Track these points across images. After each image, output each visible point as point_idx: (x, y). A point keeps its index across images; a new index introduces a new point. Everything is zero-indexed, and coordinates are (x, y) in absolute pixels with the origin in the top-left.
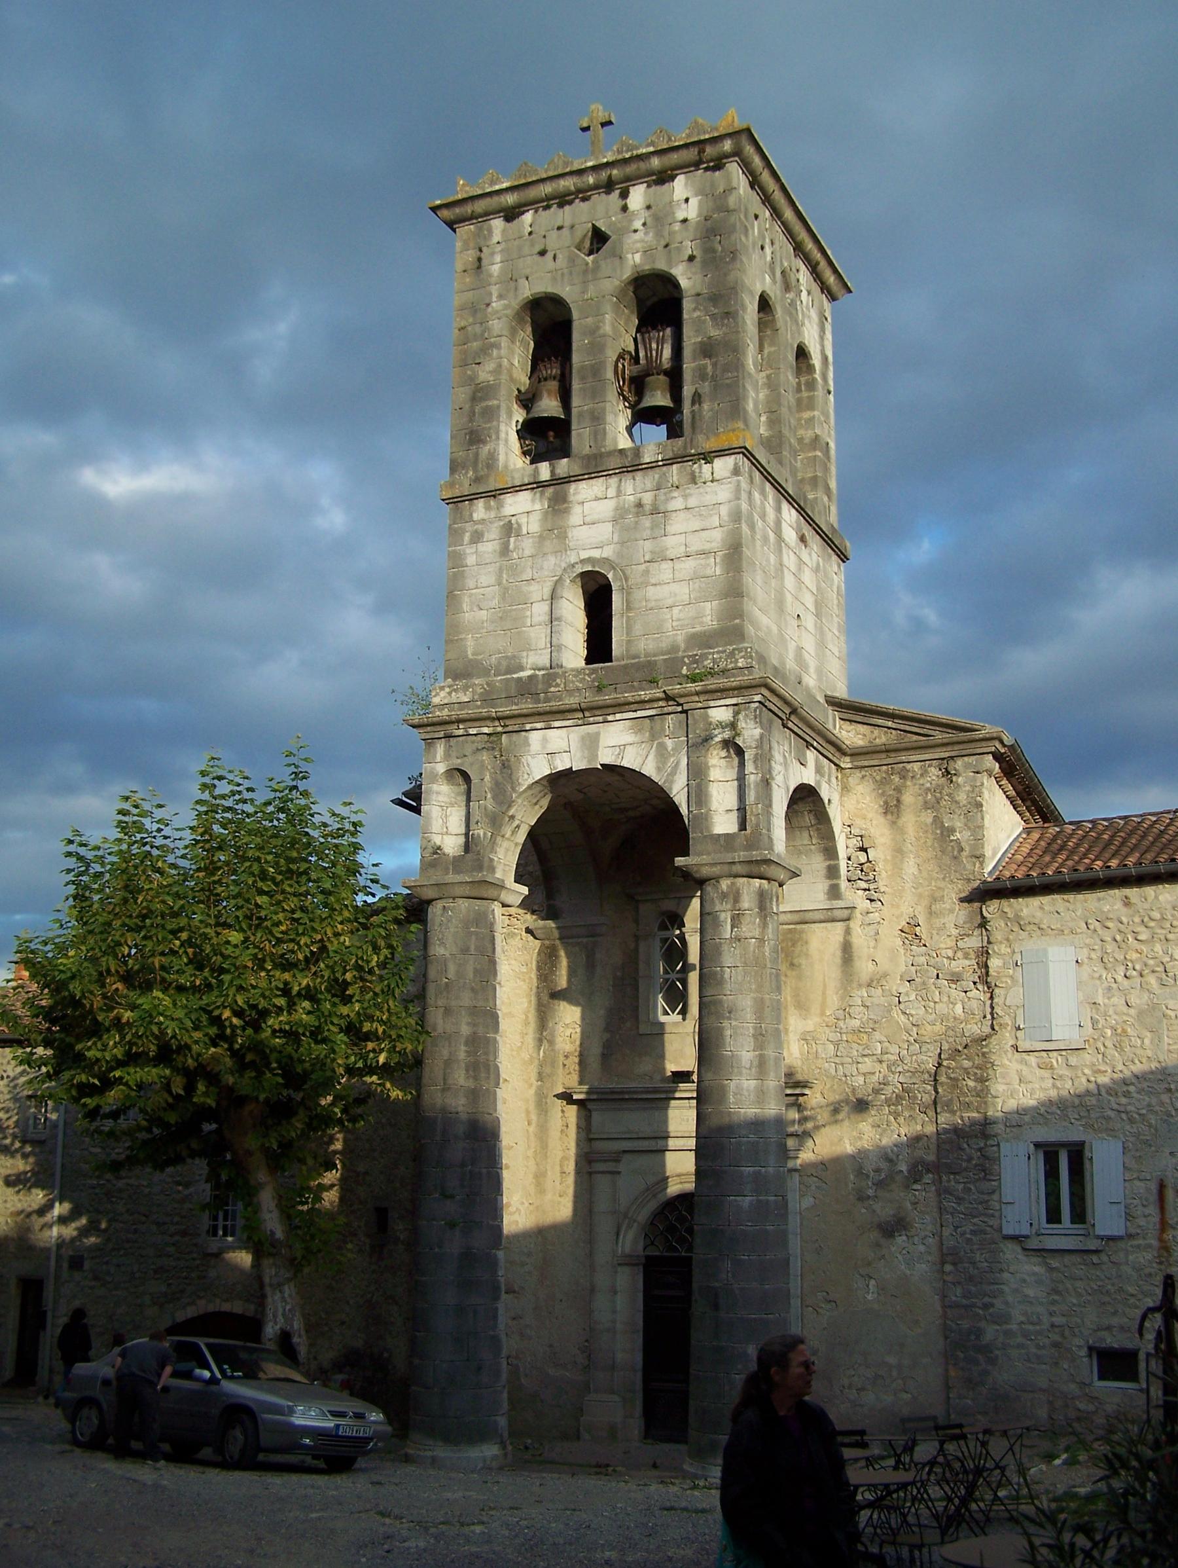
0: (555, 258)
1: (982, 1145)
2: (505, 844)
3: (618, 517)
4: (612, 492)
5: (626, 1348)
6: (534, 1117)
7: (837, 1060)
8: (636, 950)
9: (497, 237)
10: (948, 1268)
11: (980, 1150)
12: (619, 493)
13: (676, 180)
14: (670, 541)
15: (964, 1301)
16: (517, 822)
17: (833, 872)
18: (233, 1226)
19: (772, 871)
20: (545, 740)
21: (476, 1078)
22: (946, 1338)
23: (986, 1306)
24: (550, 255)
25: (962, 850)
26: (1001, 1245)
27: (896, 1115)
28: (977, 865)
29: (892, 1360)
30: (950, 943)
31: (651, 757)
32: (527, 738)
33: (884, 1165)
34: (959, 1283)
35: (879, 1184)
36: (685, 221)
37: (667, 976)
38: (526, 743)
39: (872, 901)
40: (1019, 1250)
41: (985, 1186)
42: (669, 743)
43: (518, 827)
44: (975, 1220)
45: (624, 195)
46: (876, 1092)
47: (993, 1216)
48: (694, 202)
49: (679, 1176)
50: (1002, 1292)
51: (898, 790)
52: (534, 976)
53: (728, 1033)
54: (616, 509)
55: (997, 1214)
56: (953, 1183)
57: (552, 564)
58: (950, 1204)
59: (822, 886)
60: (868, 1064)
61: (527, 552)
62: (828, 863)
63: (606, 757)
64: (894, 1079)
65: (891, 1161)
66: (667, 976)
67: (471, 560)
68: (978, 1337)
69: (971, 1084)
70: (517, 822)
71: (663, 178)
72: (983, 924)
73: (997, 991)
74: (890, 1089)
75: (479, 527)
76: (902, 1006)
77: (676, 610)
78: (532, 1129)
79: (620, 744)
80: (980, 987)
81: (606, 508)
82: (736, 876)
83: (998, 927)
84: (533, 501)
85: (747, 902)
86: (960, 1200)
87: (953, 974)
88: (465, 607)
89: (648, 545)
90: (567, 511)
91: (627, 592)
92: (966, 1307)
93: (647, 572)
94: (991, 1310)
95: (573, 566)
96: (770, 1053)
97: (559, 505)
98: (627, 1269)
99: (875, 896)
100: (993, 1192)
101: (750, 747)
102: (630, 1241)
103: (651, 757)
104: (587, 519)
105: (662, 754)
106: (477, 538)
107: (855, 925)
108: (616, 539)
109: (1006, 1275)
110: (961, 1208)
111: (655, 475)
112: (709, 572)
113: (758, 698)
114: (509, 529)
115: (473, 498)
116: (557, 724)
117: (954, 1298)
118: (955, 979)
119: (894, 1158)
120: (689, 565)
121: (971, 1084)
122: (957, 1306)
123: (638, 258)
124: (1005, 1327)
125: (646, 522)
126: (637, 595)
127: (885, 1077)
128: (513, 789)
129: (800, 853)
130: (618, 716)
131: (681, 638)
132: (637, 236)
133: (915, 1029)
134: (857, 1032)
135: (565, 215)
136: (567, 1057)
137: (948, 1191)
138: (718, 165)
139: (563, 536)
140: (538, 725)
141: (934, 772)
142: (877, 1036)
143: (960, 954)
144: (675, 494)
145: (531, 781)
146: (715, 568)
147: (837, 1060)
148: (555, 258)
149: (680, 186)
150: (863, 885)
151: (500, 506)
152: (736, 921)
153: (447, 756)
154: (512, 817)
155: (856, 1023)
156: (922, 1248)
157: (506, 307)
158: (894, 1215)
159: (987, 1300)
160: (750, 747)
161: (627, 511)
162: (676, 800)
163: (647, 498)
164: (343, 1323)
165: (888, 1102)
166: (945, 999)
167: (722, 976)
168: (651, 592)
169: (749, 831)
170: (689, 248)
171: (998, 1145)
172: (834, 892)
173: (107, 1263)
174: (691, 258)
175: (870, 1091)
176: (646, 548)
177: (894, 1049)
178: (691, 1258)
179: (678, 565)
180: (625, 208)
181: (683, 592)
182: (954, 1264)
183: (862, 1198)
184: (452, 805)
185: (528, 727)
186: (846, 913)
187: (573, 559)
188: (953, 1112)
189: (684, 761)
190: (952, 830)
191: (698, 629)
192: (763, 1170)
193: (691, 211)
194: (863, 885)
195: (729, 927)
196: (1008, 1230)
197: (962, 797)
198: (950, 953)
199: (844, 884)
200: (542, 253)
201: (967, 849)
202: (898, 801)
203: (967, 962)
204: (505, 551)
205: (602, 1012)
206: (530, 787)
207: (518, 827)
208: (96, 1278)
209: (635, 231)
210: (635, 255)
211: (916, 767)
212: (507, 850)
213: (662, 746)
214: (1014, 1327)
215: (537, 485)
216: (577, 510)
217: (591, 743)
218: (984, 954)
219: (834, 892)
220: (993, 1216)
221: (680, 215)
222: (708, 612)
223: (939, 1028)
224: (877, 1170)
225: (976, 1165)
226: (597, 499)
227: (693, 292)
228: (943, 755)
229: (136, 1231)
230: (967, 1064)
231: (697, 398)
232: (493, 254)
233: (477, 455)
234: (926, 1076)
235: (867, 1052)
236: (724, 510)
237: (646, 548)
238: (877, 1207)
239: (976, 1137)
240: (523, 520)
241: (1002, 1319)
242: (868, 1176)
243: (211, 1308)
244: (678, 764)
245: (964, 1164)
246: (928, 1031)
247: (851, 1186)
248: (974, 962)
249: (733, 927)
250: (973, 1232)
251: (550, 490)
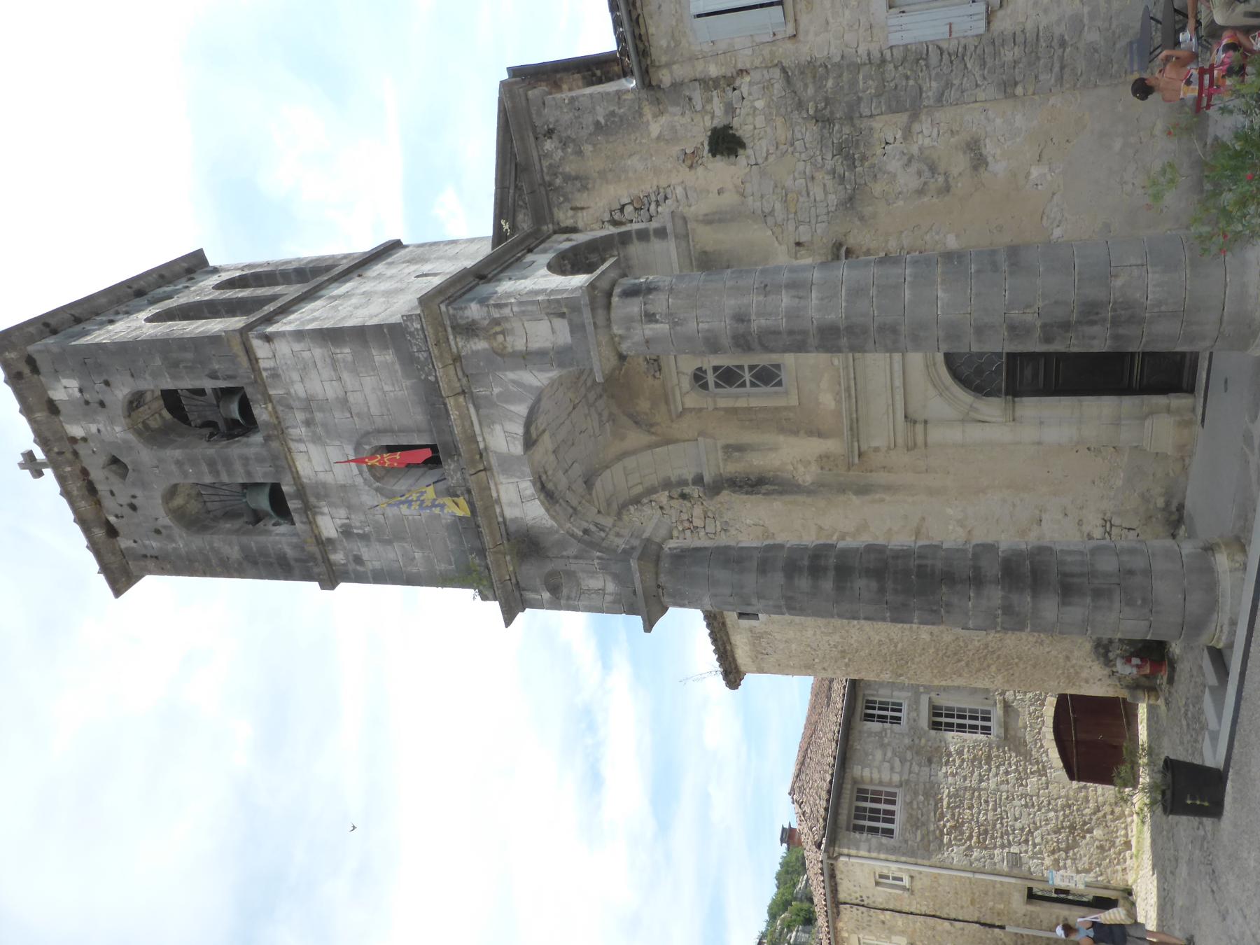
0: (134, 497)
1: (891, 66)
2: (611, 537)
3: (316, 439)
4: (302, 447)
5: (1099, 410)
6: (877, 496)
7: (813, 221)
8: (727, 410)
9: (130, 543)
10: (1019, 90)
11: (896, 68)
12: (300, 441)
13: (54, 398)
14: (330, 394)
15: (1056, 69)
16: (593, 528)
17: (643, 235)
18: (983, 712)
19: (604, 284)
20: (511, 504)
21: (825, 569)
22: (1096, 86)
23: (1063, 44)
24: (134, 501)
25: (613, 114)
26: (996, 34)
27: (864, 158)
28: (625, 97)
29: (1118, 144)
30: (698, 118)
31: (512, 408)
32: (512, 520)
33: (915, 167)
34: (1036, 77)
35: (933, 169)
36: (81, 391)
37: (748, 383)
38: (515, 520)
39: (666, 198)
40: (1000, 14)
41: (934, 59)
42: (496, 390)
43: (596, 525)
44: (969, 65)
45: (73, 440)
46: (842, 179)
47: (965, 47)
48: (65, 382)
49: (927, 367)
50: (1047, 28)
51: (568, 178)
52: (753, 497)
53: (763, 321)
54: (314, 442)
55: (963, 42)
56: (930, 94)
57: (368, 498)
58: (953, 94)
59: (656, 245)
60: (817, 191)
61: (363, 518)
62: (635, 240)
63: (517, 449)
64: (829, 164)
65: (910, 161)
66: (748, 383)
67: (377, 565)
68: (1096, 51)
69: (830, 83)
70: (593, 528)
71: (53, 408)
72: (677, 86)
73: (740, 66)
74: (840, 170)
75: (351, 558)
76: (760, 161)
77: (387, 388)
78: (888, 498)
79: (503, 438)
80: (737, 84)
81: (314, 451)
82: (609, 320)
83: (681, 72)
84: (323, 514)
85: (634, 307)
86: (949, 85)
87: (726, 112)
88: (415, 570)
89: (337, 414)
90: (324, 485)
91: (379, 432)
92: (1062, 68)
93: (358, 415)
94: (1066, 37)
95: (365, 479)
96: (785, 277)
97: (323, 491)
98: (1018, 413)
99: (662, 194)
100: (939, 48)
101: (488, 312)
102: (991, 408)
103: (512, 408)
104: (327, 468)
105: (507, 397)
106: (358, 560)
107: (690, 212)
108: (338, 443)
109: (1029, 25)
110: (956, 82)
111: (280, 408)
112: (349, 358)
113: (443, 307)
114: (347, 532)
115: (327, 561)
116: (494, 495)
117: (1053, 80)
118: (730, 109)
119: (906, 158)
120: (346, 376)
121: (830, 83)
122: (1060, 79)
123: (118, 429)
124: (1086, 21)
125: (319, 416)
126: (379, 423)
127: (828, 173)
128: (557, 532)
129: (629, 267)
130: (480, 439)
131: (407, 383)
132: (102, 429)
133: (781, 147)
134: (785, 201)
135: (102, 488)
136: (822, 468)
137: (940, 98)
138: (31, 361)
139: (343, 487)
140: (498, 510)
141: (549, 145)
142: (789, 183)
143: (708, 107)
144: (292, 391)
145: (547, 517)
146: (345, 353)
147: (813, 221)
148: (134, 497)
149: (58, 395)
150: (653, 207)
151: (330, 540)
152: (650, 317)
153: (535, 591)
154: (586, 531)
155: (778, 206)
156: (999, 121)
157: (181, 537)
158: (965, 153)
159: (1055, 43)
160: (488, 312)
161: (314, 433)
162: (546, 383)
163: (300, 416)
164: (1067, 658)
165: (853, 166)
166: (750, 119)
167: (708, 330)
168: (375, 410)
169: (565, 310)
170: (100, 386)
171: (891, 48)
172: (661, 233)
173: (1014, 830)
174: (107, 383)
175: (841, 187)
176: (339, 417)
177: (801, 166)
178: (1008, 354)
179: (350, 387)
180: (84, 439)
181: (369, 382)
182: (1016, 84)
183: (947, 189)
184: (579, 585)
185: (500, 519)
186: (680, 223)
187: (359, 480)
188: (860, 99)
189: (511, 375)
190: (597, 123)
191: (397, 367)
192: (908, 279)
193: (73, 384)
194: (653, 207)
195: (658, 326)
196: (980, 27)
197: (567, 117)
198: (707, 118)
199: (654, 225)
200: (133, 507)
201: (611, 108)
202: (577, 178)
203: (716, 100)
204: (364, 537)
205: (781, 438)
206: (553, 517)
207: (596, 525)
208: (1026, 841)
209: (99, 431)
210: (117, 431)
211: (545, 164)
212: (618, 535)
213: (499, 395)
214: (1086, 10)
215: (309, 510)
216: (322, 476)
217: (508, 463)
218: (709, 84)
219: (661, 233)
220: (965, 47)
221: (78, 395)
222: (382, 358)
223: (779, 121)
224: (920, 174)
225: (911, 70)
226: (309, 460)
227: (130, 380)
228: (532, 139)
229: (987, 802)
230: (811, 91)
231: (213, 376)
232: (145, 546)
233: (297, 560)
234: (825, 131)
235: (804, 193)
236: (297, 347)
237: (339, 417)
238: (955, 171)
239: (883, 73)
240: (339, 522)
241: (1077, 24)
242: (925, 183)
243: (1051, 736)
244: (514, 382)
245: (911, 82)
246: (782, 134)
247: (935, 200)
248: (715, 93)
249: (657, 321)
250: (983, 64)
251: (312, 500)
